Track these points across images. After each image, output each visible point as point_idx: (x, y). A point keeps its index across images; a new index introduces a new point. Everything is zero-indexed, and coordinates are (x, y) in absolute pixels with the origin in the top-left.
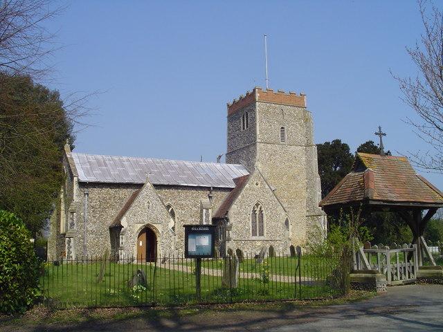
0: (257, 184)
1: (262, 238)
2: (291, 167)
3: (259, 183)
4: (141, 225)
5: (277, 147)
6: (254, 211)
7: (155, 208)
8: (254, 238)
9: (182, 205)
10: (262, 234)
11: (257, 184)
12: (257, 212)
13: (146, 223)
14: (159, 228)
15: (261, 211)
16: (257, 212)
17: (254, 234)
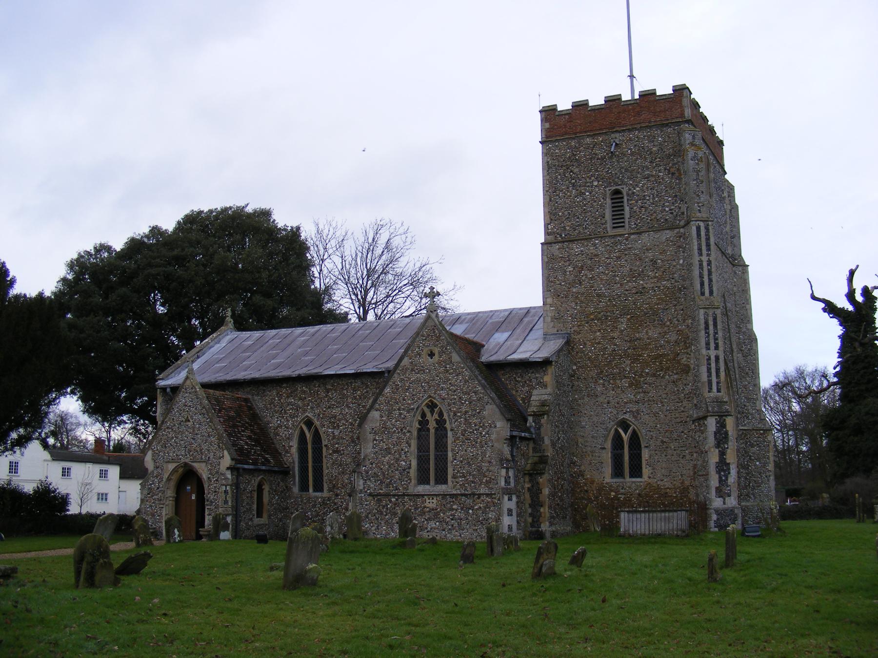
0: (432, 355)
1: (441, 488)
2: (641, 292)
3: (436, 351)
4: (175, 465)
5: (600, 247)
6: (424, 423)
7: (199, 429)
8: (421, 489)
9: (335, 417)
10: (442, 479)
11: (432, 355)
12: (432, 425)
13: (182, 461)
14: (203, 470)
15: (441, 423)
16: (432, 425)
17: (423, 479)
